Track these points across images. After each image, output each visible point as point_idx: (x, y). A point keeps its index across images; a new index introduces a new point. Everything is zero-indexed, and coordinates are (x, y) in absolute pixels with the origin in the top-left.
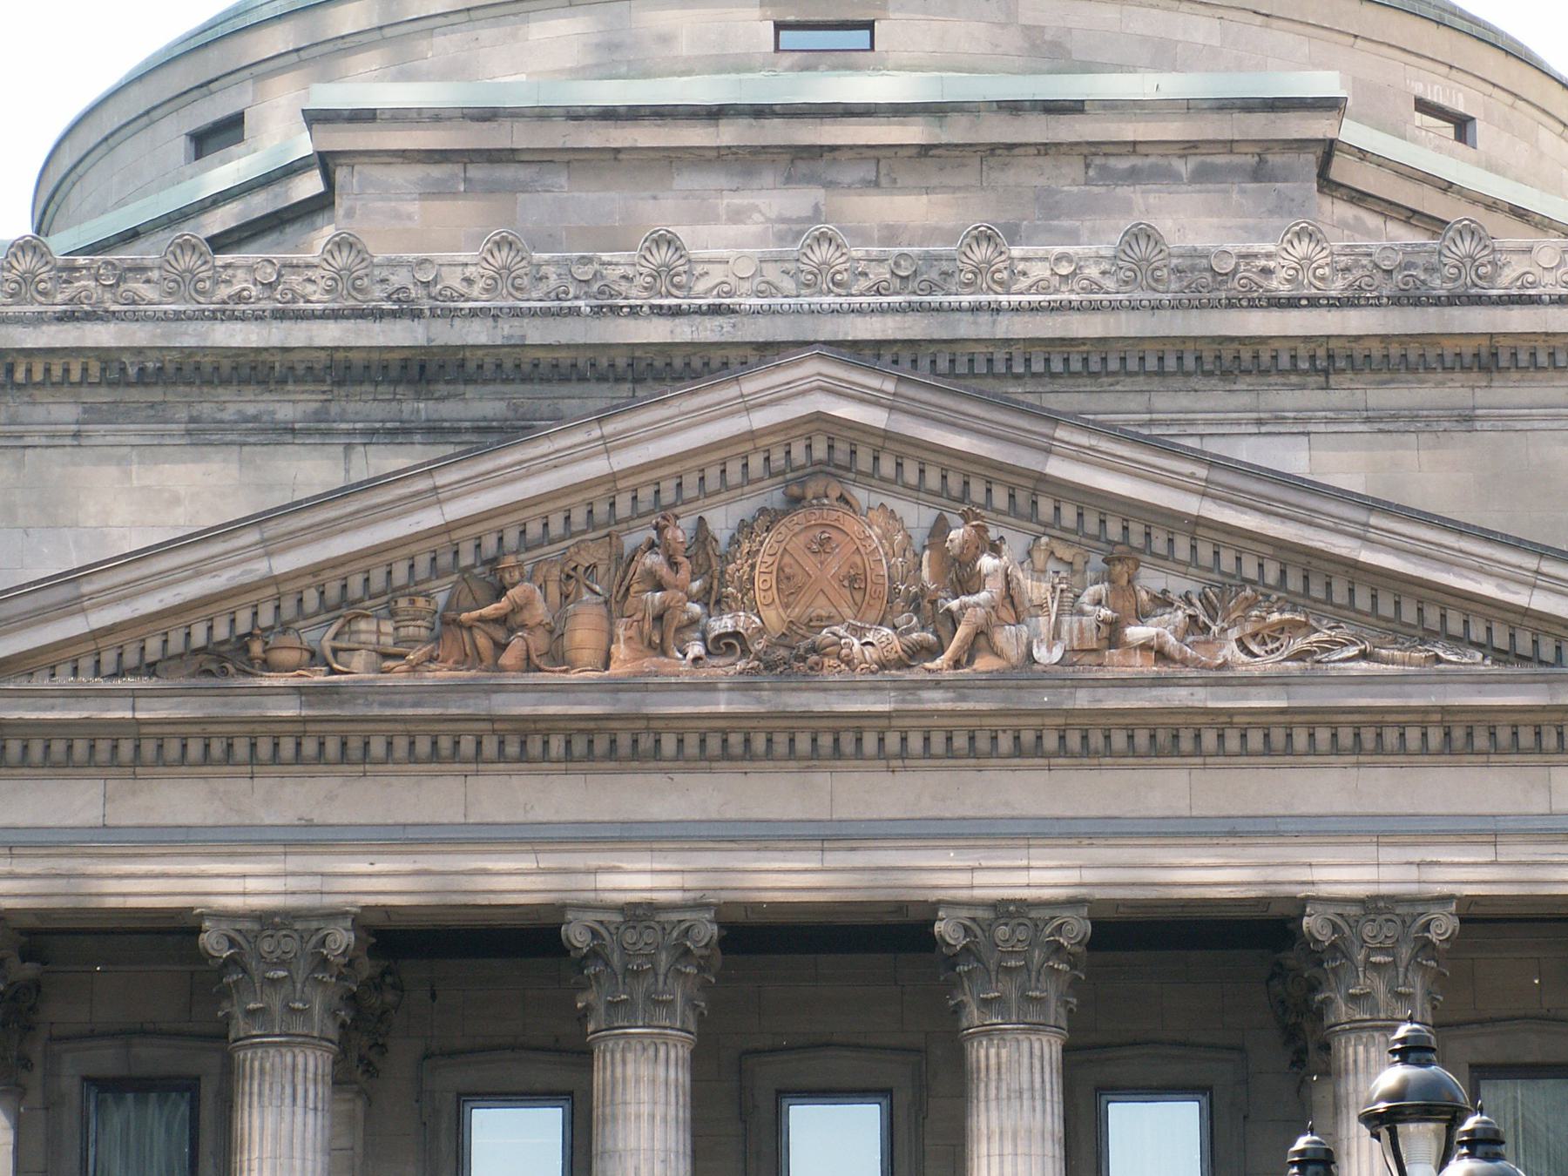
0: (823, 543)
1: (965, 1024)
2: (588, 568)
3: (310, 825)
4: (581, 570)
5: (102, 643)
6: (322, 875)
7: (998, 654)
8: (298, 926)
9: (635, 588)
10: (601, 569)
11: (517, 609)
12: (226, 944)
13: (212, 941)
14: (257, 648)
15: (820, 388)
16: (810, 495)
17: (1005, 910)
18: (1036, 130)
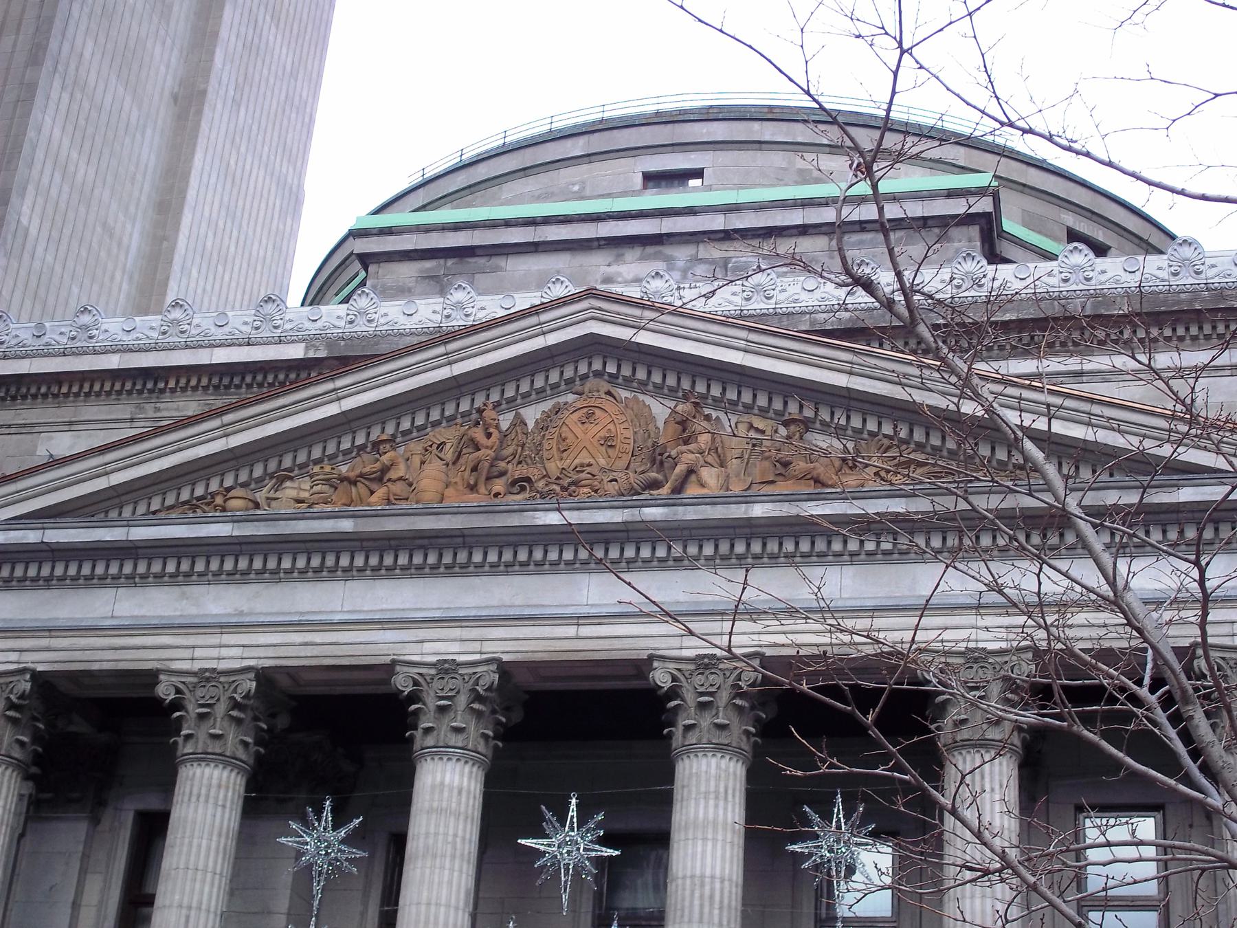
0: (590, 416)
1: (674, 746)
2: (439, 445)
3: (241, 613)
4: (435, 446)
5: (124, 498)
6: (244, 646)
7: (703, 485)
8: (222, 679)
9: (464, 451)
10: (448, 445)
11: (385, 470)
12: (173, 691)
14: (219, 500)
15: (593, 318)
16: (586, 390)
18: (796, 218)
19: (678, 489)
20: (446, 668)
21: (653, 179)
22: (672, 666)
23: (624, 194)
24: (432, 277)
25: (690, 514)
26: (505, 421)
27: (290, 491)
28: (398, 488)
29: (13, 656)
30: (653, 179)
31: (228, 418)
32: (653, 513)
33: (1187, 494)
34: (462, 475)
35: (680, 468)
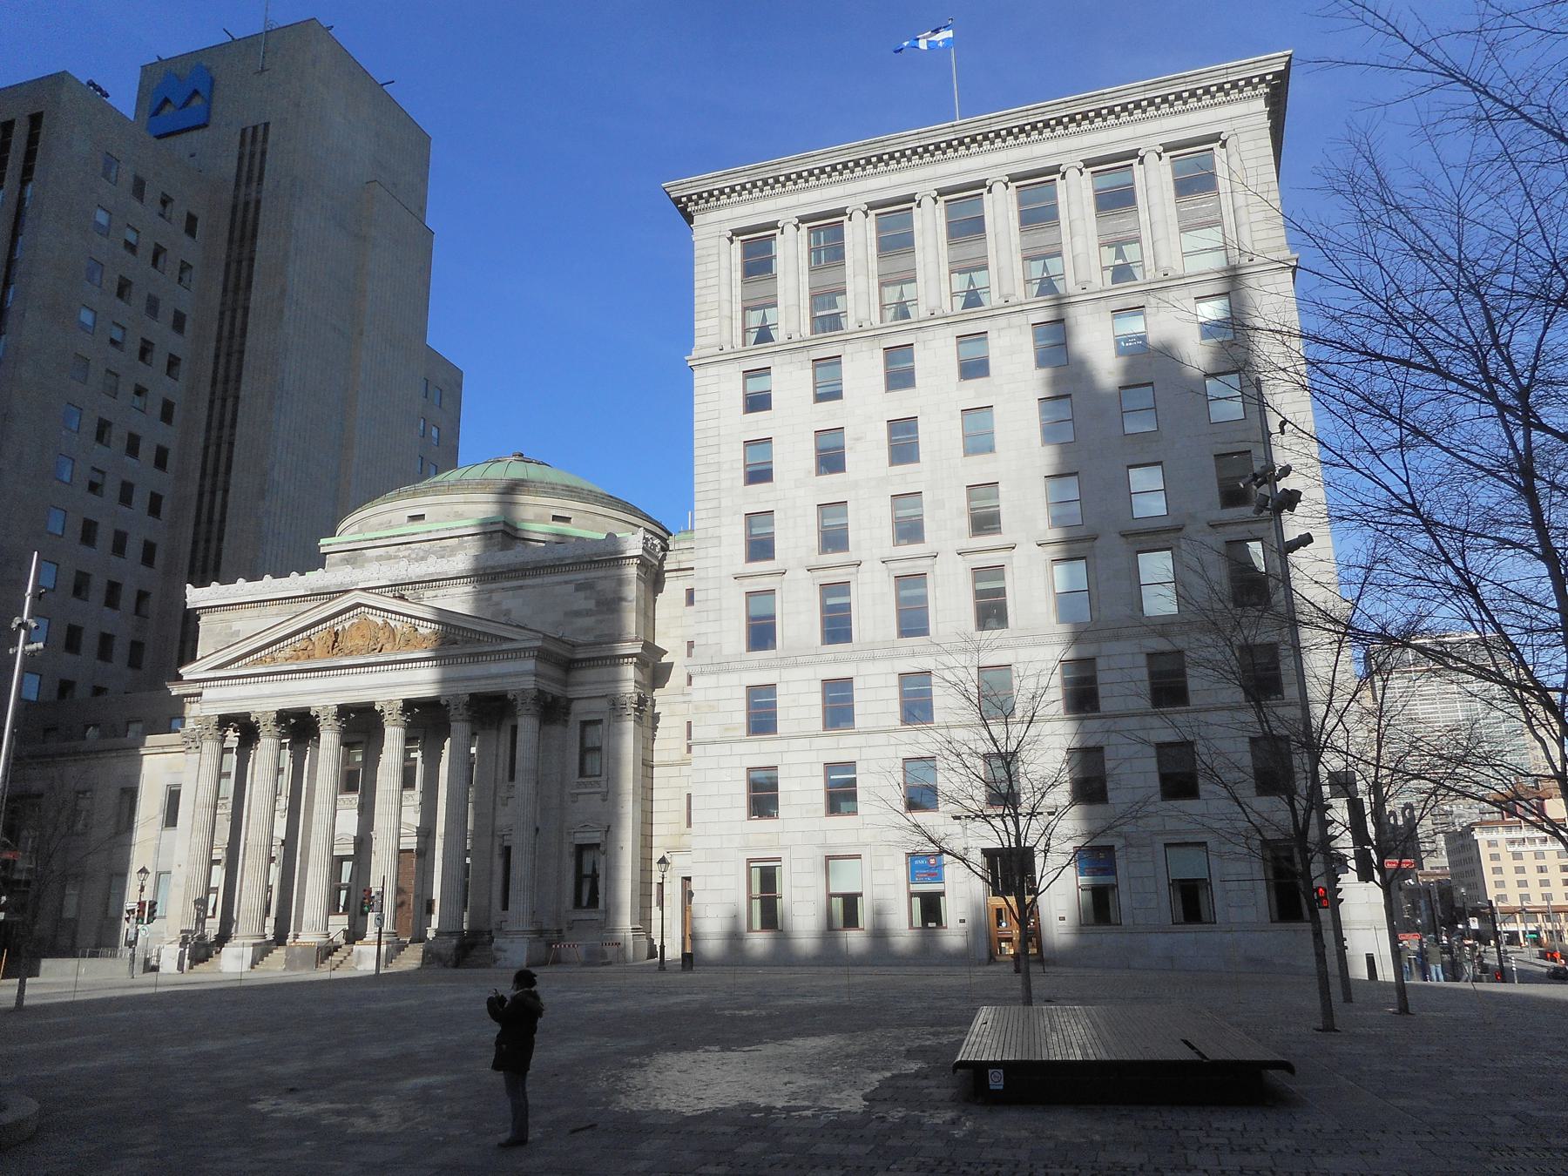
13: (253, 719)
17: (390, 702)
19: (380, 651)
20: (325, 707)
21: (414, 518)
22: (381, 703)
23: (400, 525)
24: (347, 561)
25: (382, 659)
26: (340, 628)
27: (282, 655)
28: (310, 653)
29: (214, 710)
30: (414, 518)
31: (262, 635)
32: (373, 660)
33: (505, 646)
34: (325, 650)
35: (380, 645)
